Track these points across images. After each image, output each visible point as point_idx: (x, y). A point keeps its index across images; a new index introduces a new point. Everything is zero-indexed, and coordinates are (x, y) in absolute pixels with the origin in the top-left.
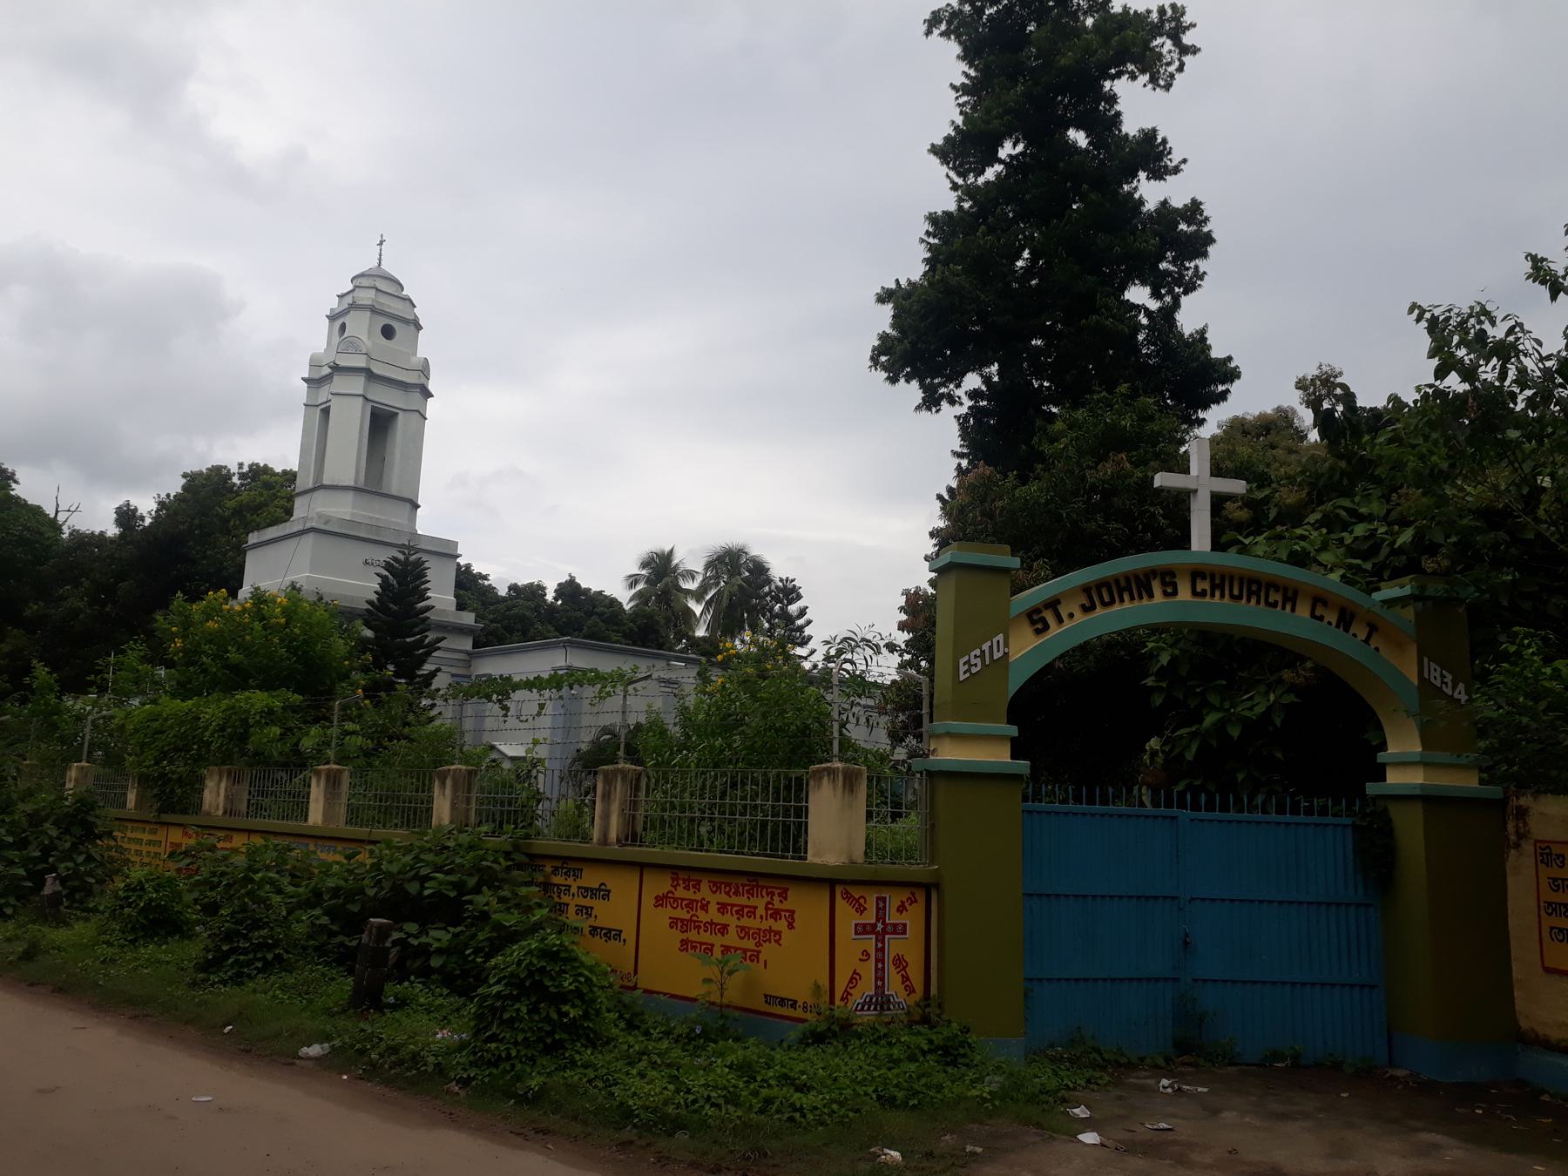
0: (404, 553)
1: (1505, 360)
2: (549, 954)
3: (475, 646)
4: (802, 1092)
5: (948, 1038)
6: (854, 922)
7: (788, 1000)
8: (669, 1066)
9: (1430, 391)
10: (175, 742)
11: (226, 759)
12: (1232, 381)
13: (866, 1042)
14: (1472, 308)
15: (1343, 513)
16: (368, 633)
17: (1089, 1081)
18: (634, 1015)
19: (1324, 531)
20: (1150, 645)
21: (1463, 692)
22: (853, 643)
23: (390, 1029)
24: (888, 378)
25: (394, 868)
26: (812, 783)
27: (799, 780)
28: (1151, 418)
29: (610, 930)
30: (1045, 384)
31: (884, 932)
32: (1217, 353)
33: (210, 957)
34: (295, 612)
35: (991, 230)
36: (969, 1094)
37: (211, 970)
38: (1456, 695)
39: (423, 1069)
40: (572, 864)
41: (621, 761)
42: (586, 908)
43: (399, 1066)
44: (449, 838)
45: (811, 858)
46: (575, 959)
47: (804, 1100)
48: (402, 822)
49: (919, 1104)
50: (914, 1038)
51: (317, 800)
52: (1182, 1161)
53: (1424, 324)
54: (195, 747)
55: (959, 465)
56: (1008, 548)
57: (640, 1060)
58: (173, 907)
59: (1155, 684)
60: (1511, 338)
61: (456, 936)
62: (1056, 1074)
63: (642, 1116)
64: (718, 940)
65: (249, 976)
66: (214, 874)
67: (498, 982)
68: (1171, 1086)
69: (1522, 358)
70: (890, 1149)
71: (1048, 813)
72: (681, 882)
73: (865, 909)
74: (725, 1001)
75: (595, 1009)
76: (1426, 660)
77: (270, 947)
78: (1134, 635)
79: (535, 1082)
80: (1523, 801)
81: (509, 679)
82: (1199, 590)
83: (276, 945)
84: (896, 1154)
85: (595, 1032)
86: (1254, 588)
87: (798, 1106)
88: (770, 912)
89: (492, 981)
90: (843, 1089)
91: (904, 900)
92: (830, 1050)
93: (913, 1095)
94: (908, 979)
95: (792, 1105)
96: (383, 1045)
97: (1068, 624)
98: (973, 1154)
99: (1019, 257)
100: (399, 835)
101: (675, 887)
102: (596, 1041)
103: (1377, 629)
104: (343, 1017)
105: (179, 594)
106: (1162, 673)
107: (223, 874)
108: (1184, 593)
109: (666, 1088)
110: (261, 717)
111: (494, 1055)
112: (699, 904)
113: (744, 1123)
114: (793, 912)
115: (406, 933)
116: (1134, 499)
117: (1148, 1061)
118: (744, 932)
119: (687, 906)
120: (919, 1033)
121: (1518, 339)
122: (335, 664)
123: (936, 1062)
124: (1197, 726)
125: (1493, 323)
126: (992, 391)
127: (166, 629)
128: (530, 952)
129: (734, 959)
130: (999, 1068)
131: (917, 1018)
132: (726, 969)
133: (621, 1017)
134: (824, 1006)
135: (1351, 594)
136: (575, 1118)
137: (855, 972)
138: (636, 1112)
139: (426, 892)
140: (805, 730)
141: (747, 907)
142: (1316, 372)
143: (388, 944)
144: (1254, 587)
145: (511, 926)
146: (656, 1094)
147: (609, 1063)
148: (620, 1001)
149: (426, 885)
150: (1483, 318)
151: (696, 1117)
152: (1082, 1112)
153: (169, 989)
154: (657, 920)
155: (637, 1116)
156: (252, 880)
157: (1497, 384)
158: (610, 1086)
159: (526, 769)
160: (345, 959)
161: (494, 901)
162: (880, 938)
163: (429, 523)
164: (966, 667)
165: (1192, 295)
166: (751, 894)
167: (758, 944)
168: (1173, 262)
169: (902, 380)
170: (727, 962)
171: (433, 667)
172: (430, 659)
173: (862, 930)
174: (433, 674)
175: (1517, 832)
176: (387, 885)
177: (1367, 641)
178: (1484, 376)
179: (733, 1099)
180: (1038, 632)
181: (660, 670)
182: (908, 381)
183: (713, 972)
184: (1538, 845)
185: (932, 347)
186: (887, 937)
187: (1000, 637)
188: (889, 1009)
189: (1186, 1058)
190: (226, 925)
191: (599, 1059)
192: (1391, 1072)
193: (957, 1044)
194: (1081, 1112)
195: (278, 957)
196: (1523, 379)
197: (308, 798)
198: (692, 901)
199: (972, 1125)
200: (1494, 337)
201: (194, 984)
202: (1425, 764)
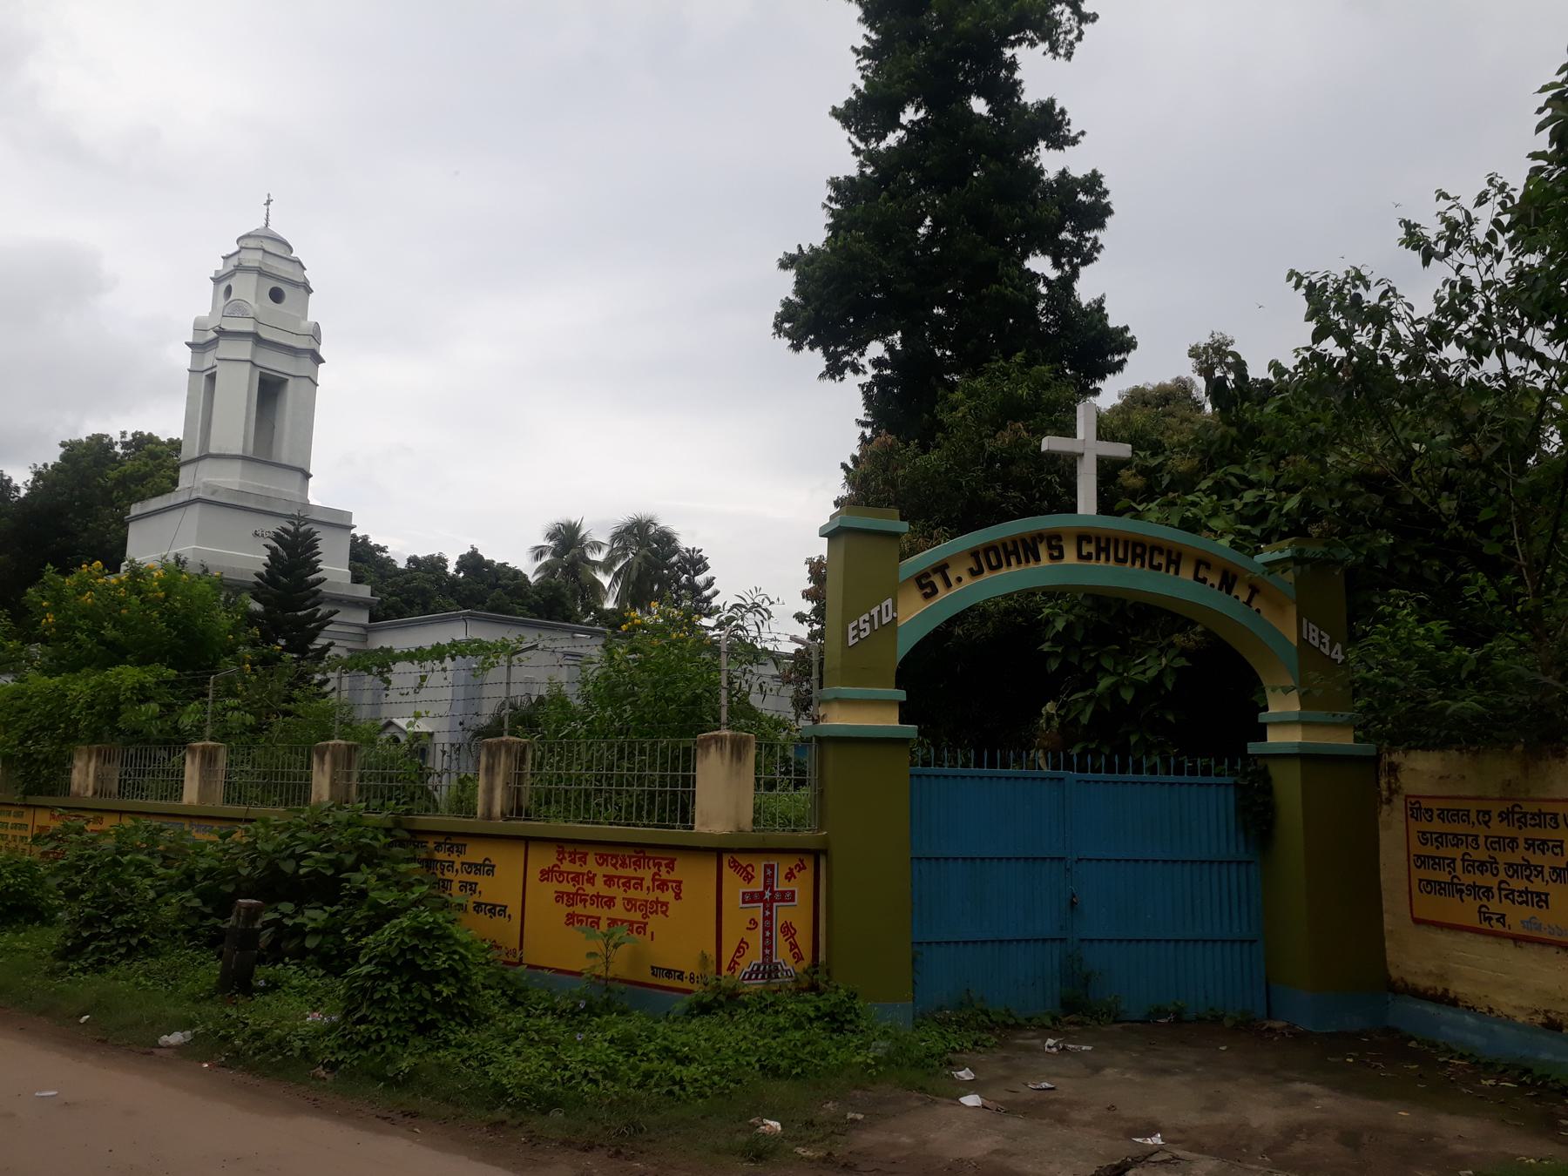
0: (293, 524)
1: (1380, 325)
2: (419, 932)
3: (371, 620)
4: (683, 1064)
5: (835, 1005)
6: (741, 891)
7: (675, 971)
8: (548, 1042)
9: (1307, 355)
10: (40, 721)
11: (96, 736)
14: (1348, 273)
15: (1233, 480)
16: (256, 606)
17: (976, 1043)
18: (519, 991)
19: (1215, 497)
20: (1047, 611)
21: (1340, 653)
23: (258, 1014)
25: (269, 848)
26: (699, 751)
27: (687, 750)
28: (1047, 386)
29: (494, 906)
31: (772, 899)
33: (69, 944)
34: (174, 584)
35: (892, 197)
36: (854, 1060)
37: (69, 957)
38: (1333, 656)
39: (289, 1054)
40: (455, 839)
41: (506, 733)
42: (471, 884)
43: (264, 1052)
44: (327, 815)
45: (697, 827)
46: (450, 937)
47: (685, 1073)
48: (281, 800)
49: (803, 1072)
51: (192, 778)
52: (1062, 1120)
53: (1302, 291)
54: (62, 725)
55: (863, 433)
56: (897, 512)
57: (517, 1038)
58: (33, 893)
59: (1050, 650)
60: (1384, 303)
61: (333, 915)
63: (517, 1095)
64: (604, 913)
65: (111, 962)
66: (81, 857)
67: (369, 962)
68: (1056, 1045)
69: (1395, 322)
70: (770, 1119)
71: (937, 776)
72: (566, 855)
73: (753, 877)
74: (610, 975)
75: (470, 987)
77: (134, 932)
78: (1031, 601)
79: (405, 1065)
80: (1395, 758)
81: (390, 650)
82: (1084, 553)
83: (139, 930)
84: (776, 1124)
85: (471, 1010)
86: (1139, 550)
87: (678, 1079)
88: (657, 883)
89: (362, 961)
90: (725, 1060)
91: (793, 867)
92: (716, 1020)
93: (797, 1063)
94: (796, 946)
95: (673, 1078)
96: (248, 1031)
97: (956, 588)
100: (276, 814)
101: (561, 860)
102: (472, 1019)
104: (209, 1003)
105: (49, 566)
106: (1058, 639)
107: (91, 857)
108: (1070, 557)
109: (542, 1065)
110: (132, 693)
111: (363, 1037)
112: (586, 877)
113: (621, 1098)
114: (680, 882)
115: (281, 914)
117: (1035, 1021)
118: (631, 904)
119: (573, 879)
121: (1391, 304)
122: (217, 639)
123: (824, 1029)
125: (1367, 287)
127: (36, 602)
128: (402, 930)
129: (621, 932)
130: (885, 1033)
131: (805, 985)
132: (612, 943)
133: (504, 993)
134: (711, 977)
135: (1237, 558)
136: (447, 1100)
137: (742, 941)
138: (510, 1091)
139: (302, 871)
140: (696, 700)
141: (634, 878)
143: (258, 926)
144: (1139, 550)
145: (389, 904)
146: (531, 1072)
147: (485, 1041)
148: (503, 978)
149: (302, 863)
150: (1357, 282)
151: (571, 1093)
152: (967, 1074)
153: (24, 979)
154: (544, 894)
155: (511, 1095)
156: (120, 864)
157: (1372, 348)
158: (485, 1065)
159: (420, 746)
160: (215, 940)
161: (373, 880)
162: (768, 906)
163: (319, 494)
164: (855, 632)
166: (637, 865)
167: (645, 916)
170: (613, 934)
171: (326, 642)
172: (323, 633)
173: (750, 898)
174: (326, 648)
175: (1389, 788)
176: (261, 864)
177: (1248, 603)
178: (1358, 340)
179: (611, 1074)
180: (927, 596)
181: (563, 642)
183: (597, 945)
186: (775, 904)
187: (889, 602)
188: (777, 977)
189: (1072, 1018)
190: (87, 910)
191: (474, 1038)
192: (1269, 1024)
193: (844, 1010)
194: (965, 1075)
195: (143, 943)
196: (1396, 342)
197: (183, 776)
198: (578, 874)
199: (855, 1092)
200: (1369, 302)
201: (53, 973)
202: (1304, 723)
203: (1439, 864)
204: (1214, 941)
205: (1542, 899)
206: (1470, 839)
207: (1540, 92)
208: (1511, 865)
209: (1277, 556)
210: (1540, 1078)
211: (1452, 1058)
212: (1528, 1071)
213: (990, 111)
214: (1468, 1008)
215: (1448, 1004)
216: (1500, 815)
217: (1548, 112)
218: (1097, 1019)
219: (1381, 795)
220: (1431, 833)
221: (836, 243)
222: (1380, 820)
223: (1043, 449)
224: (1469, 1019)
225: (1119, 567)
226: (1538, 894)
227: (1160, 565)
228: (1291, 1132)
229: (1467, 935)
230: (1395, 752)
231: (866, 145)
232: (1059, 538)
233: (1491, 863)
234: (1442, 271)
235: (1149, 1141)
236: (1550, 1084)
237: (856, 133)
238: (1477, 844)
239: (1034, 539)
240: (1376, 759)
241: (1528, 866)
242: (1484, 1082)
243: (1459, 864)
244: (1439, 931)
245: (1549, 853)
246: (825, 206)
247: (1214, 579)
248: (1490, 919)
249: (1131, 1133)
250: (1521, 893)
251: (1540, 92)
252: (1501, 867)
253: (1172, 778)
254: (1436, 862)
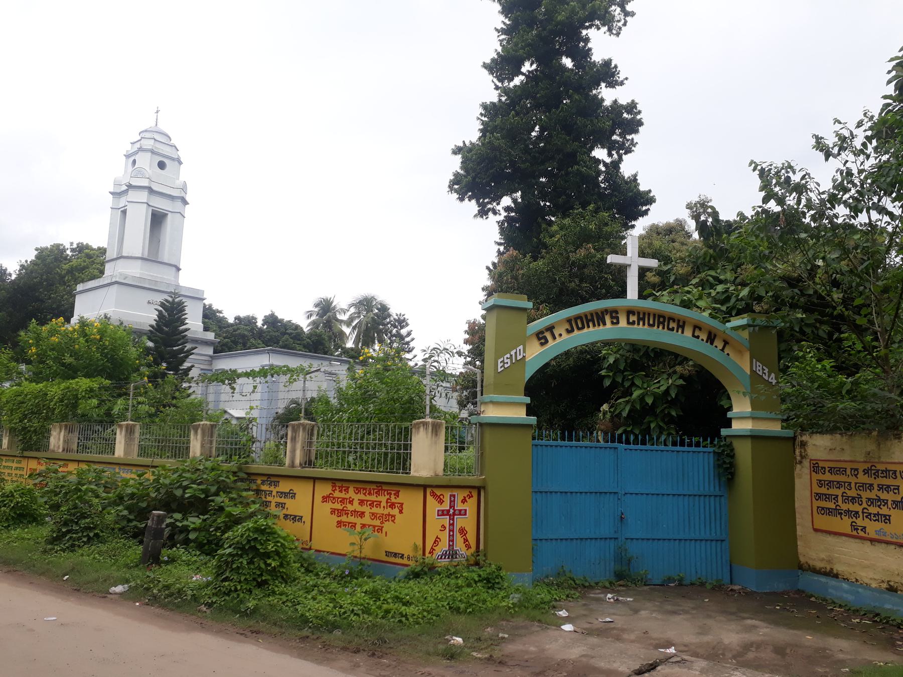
0: (172, 297)
1: (800, 194)
2: (258, 530)
3: (214, 353)
4: (407, 606)
5: (489, 574)
6: (437, 509)
7: (399, 554)
8: (330, 593)
9: (760, 210)
10: (32, 409)
11: (64, 418)
12: (651, 204)
13: (443, 577)
14: (783, 164)
15: (711, 279)
16: (150, 344)
17: (568, 596)
18: (310, 564)
19: (700, 288)
20: (604, 352)
21: (774, 378)
22: (438, 351)
23: (164, 575)
25: (167, 481)
26: (414, 430)
27: (406, 429)
28: (606, 224)
29: (295, 516)
30: (548, 204)
31: (454, 514)
32: (643, 188)
33: (55, 535)
34: (106, 331)
35: (517, 114)
36: (501, 605)
37: (55, 543)
38: (770, 380)
39: (185, 598)
40: (272, 478)
41: (302, 419)
42: (282, 504)
43: (171, 596)
44: (200, 464)
45: (413, 473)
46: (275, 533)
48: (172, 455)
50: (470, 574)
51: (120, 442)
52: (618, 639)
53: (757, 172)
54: (45, 411)
55: (499, 249)
56: (526, 297)
57: (313, 590)
58: (31, 506)
59: (606, 374)
60: (803, 182)
61: (204, 520)
62: (550, 593)
63: (314, 622)
64: (359, 521)
65: (79, 546)
66: (57, 487)
67: (230, 547)
68: (613, 598)
69: (809, 193)
70: (456, 636)
71: (546, 446)
72: (337, 488)
73: (443, 501)
74: (363, 555)
75: (287, 562)
76: (754, 360)
77: (90, 529)
78: (595, 346)
79: (251, 604)
80: (804, 438)
81: (235, 371)
82: (631, 321)
83: (94, 528)
84: (460, 640)
85: (287, 575)
86: (661, 320)
87: (404, 614)
88: (389, 504)
89: (226, 546)
90: (430, 603)
91: (466, 496)
92: (423, 581)
93: (470, 606)
94: (467, 541)
95: (401, 613)
96: (160, 585)
97: (558, 340)
98: (503, 638)
99: (533, 130)
100: (170, 463)
101: (334, 491)
102: (287, 579)
103: (728, 343)
104: (136, 569)
105: (33, 320)
106: (610, 368)
107: (63, 486)
108: (623, 323)
109: (328, 606)
110: (86, 393)
111: (227, 589)
112: (348, 500)
113: (373, 624)
115: (174, 519)
116: (596, 270)
117: (600, 584)
118: (374, 516)
119: (341, 501)
120: (473, 571)
121: (807, 182)
122: (130, 363)
123: (483, 587)
124: (629, 397)
125: (794, 173)
126: (517, 207)
127: (26, 341)
128: (249, 529)
129: (368, 531)
130: (518, 590)
131: (472, 562)
132: (364, 537)
133: (302, 566)
134: (420, 557)
135: (715, 324)
136: (275, 624)
138: (311, 620)
139: (187, 496)
140: (411, 401)
141: (376, 501)
142: (698, 199)
143: (164, 526)
144: (662, 320)
145: (237, 515)
146: (322, 609)
147: (295, 592)
148: (301, 557)
149: (187, 491)
150: (789, 170)
151: (345, 621)
152: (564, 613)
153: (29, 555)
154: (324, 510)
155: (311, 622)
156: (80, 490)
157: (795, 207)
158: (295, 605)
159: (246, 424)
160: (138, 535)
161: (227, 500)
162: (452, 518)
163: (187, 280)
165: (629, 155)
166: (378, 494)
167: (382, 523)
168: (620, 135)
170: (364, 533)
171: (189, 365)
172: (188, 360)
173: (442, 513)
174: (189, 369)
175: (801, 455)
176: (163, 491)
177: (723, 350)
178: (788, 203)
179: (367, 611)
180: (542, 344)
181: (325, 366)
183: (356, 539)
184: (812, 462)
186: (455, 517)
187: (521, 347)
188: (456, 558)
189: (621, 582)
190: (65, 516)
191: (289, 590)
193: (494, 576)
194: (563, 613)
195: (96, 535)
196: (809, 206)
197: (115, 441)
198: (344, 499)
199: (502, 622)
200: (794, 181)
201: (45, 552)
202: (754, 418)
205: (887, 519)
206: (846, 484)
208: (869, 499)
210: (885, 618)
211: (835, 607)
212: (877, 615)
214: (843, 579)
215: (833, 577)
216: (864, 471)
219: (796, 459)
220: (825, 481)
221: (485, 140)
222: (796, 473)
223: (608, 262)
224: (845, 586)
226: (885, 516)
228: (747, 647)
229: (844, 538)
232: (617, 312)
233: (858, 498)
234: (835, 164)
238: (850, 487)
239: (602, 313)
240: (794, 439)
241: (879, 500)
242: (853, 620)
243: (840, 498)
244: (828, 536)
246: (478, 119)
247: (704, 336)
249: (657, 647)
252: (864, 500)
254: (827, 497)
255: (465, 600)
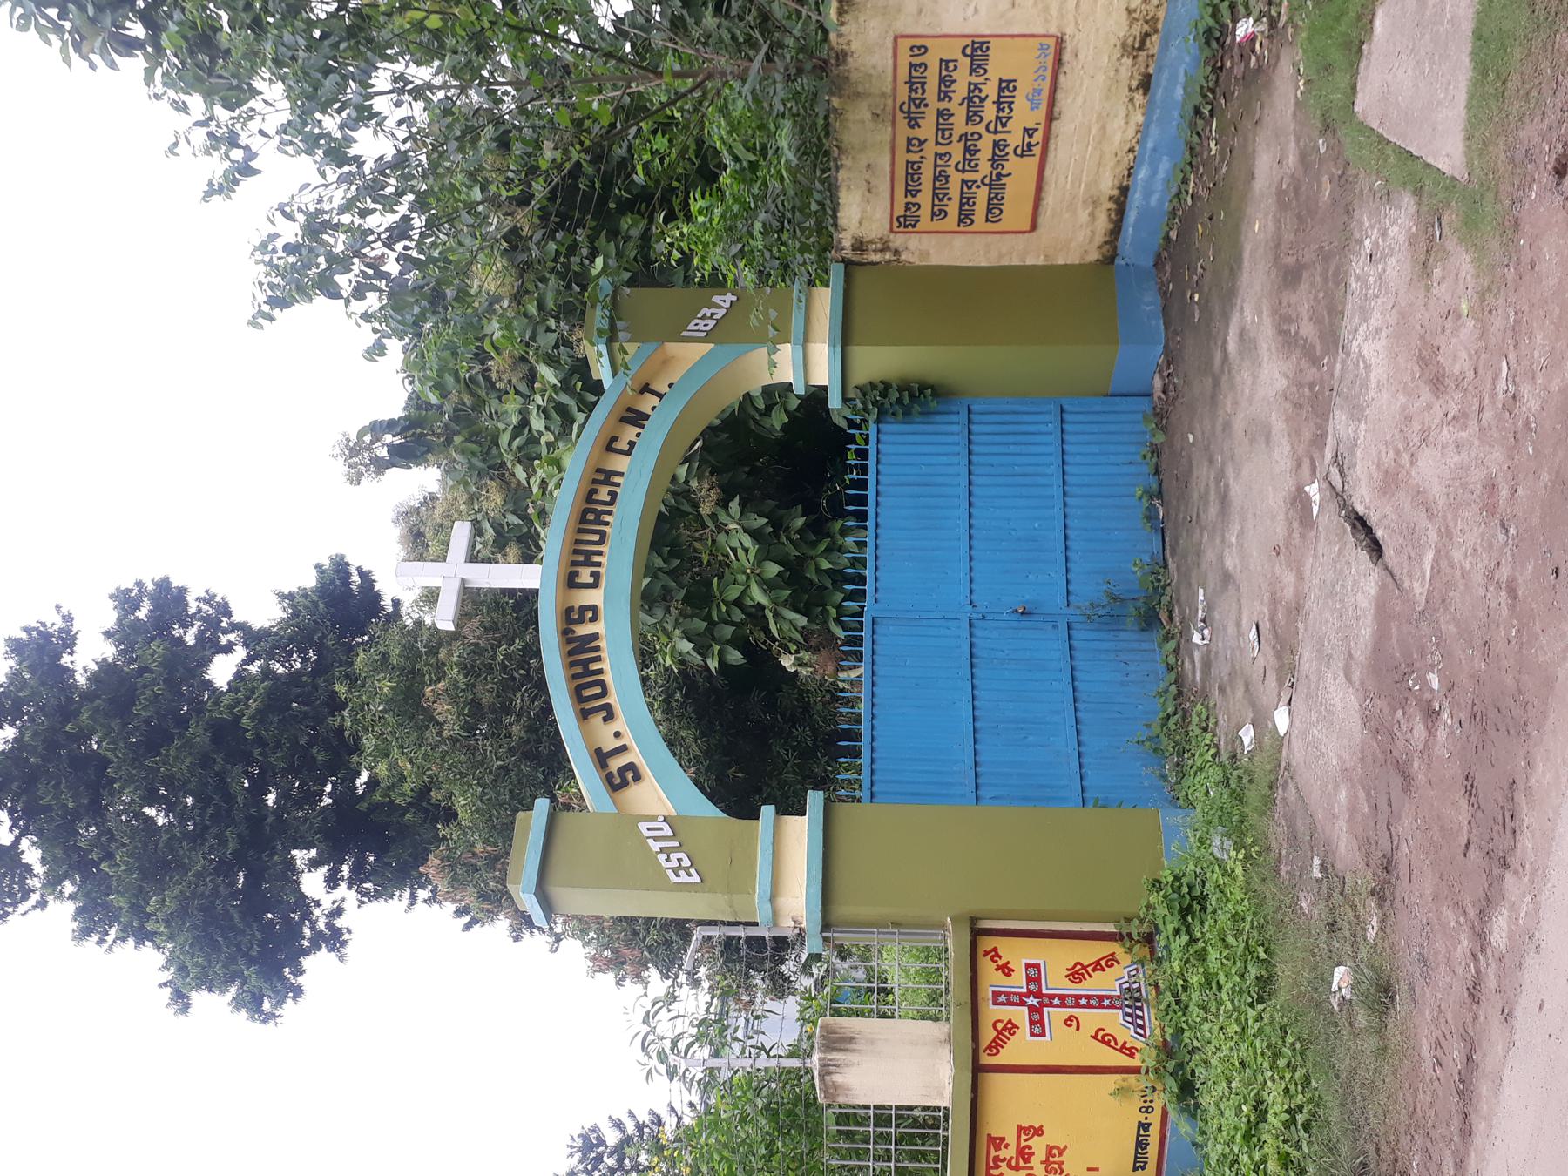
5: (1170, 908)
7: (1139, 1135)
12: (347, 564)
13: (1187, 1022)
14: (258, 262)
15: (517, 442)
17: (1205, 729)
19: (537, 462)
20: (668, 662)
21: (723, 298)
22: (651, 1037)
24: (294, 998)
28: (385, 656)
30: (329, 788)
31: (1038, 994)
32: (310, 581)
35: (109, 856)
45: (944, 1102)
49: (1263, 945)
50: (1174, 954)
53: (276, 312)
55: (425, 901)
56: (520, 815)
59: (716, 659)
60: (301, 218)
62: (1202, 769)
68: (1201, 631)
73: (1010, 1022)
76: (684, 334)
78: (656, 682)
80: (847, 243)
82: (591, 580)
88: (1022, 1164)
91: (994, 966)
94: (1098, 963)
97: (628, 739)
98: (1323, 868)
99: (150, 821)
103: (648, 384)
106: (702, 650)
108: (593, 597)
114: (1020, 1128)
116: (485, 679)
117: (1172, 660)
120: (1167, 947)
121: (300, 210)
124: (767, 611)
125: (276, 236)
126: (330, 856)
134: (1143, 1081)
137: (1095, 1037)
142: (341, 460)
144: (590, 516)
150: (270, 247)
162: (1046, 1000)
164: (682, 873)
165: (232, 606)
168: (185, 626)
169: (300, 980)
173: (1038, 1025)
175: (882, 251)
177: (660, 396)
180: (637, 777)
182: (302, 972)
184: (895, 229)
185: (258, 935)
187: (643, 826)
188: (1139, 990)
189: (1164, 617)
192: (1158, 392)
193: (1175, 896)
194: (1247, 735)
199: (1283, 873)
202: (806, 341)
203: (969, 199)
204: (1063, 452)
205: (1006, 86)
206: (939, 162)
207: (69, 65)
208: (969, 119)
209: (605, 360)
210: (1205, 96)
211: (1187, 192)
212: (1197, 111)
213: (12, 724)
214: (1129, 175)
215: (1126, 197)
216: (912, 127)
217: (95, 58)
218: (1164, 588)
219: (890, 261)
220: (933, 205)
221: (161, 934)
222: (918, 263)
223: (453, 628)
224: (1142, 174)
225: (609, 542)
226: (1001, 90)
227: (610, 493)
229: (1048, 172)
230: (839, 242)
231: (33, 891)
232: (569, 610)
233: (967, 140)
234: (268, 155)
235: (1316, 498)
236: (1211, 84)
237: (15, 905)
238: (945, 155)
239: (569, 641)
240: (848, 263)
241: (970, 99)
242: (1213, 152)
243: (968, 176)
244: (1044, 203)
245: (955, 75)
246: (110, 949)
247: (630, 432)
248: (1029, 144)
250: (999, 109)
251: (69, 65)
252: (971, 129)
253: (870, 523)
254: (966, 202)
255: (1238, 964)
